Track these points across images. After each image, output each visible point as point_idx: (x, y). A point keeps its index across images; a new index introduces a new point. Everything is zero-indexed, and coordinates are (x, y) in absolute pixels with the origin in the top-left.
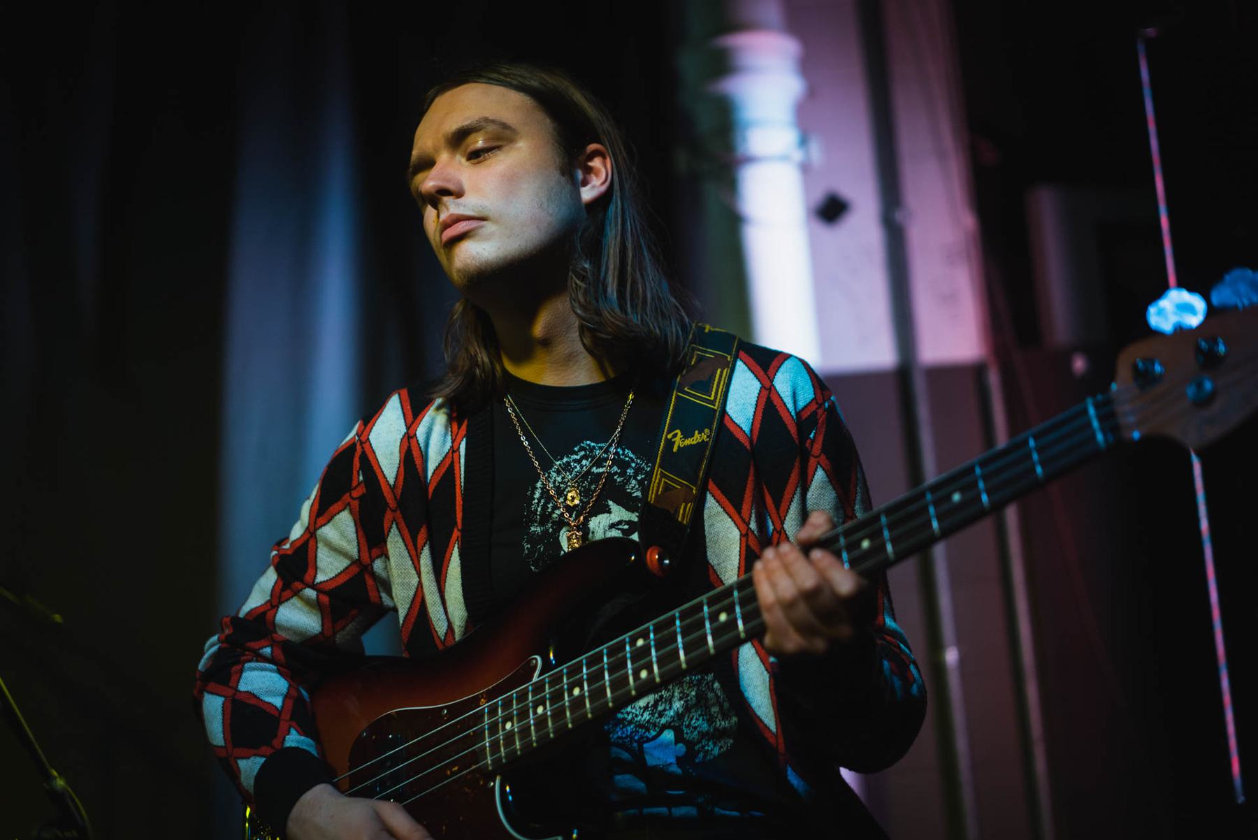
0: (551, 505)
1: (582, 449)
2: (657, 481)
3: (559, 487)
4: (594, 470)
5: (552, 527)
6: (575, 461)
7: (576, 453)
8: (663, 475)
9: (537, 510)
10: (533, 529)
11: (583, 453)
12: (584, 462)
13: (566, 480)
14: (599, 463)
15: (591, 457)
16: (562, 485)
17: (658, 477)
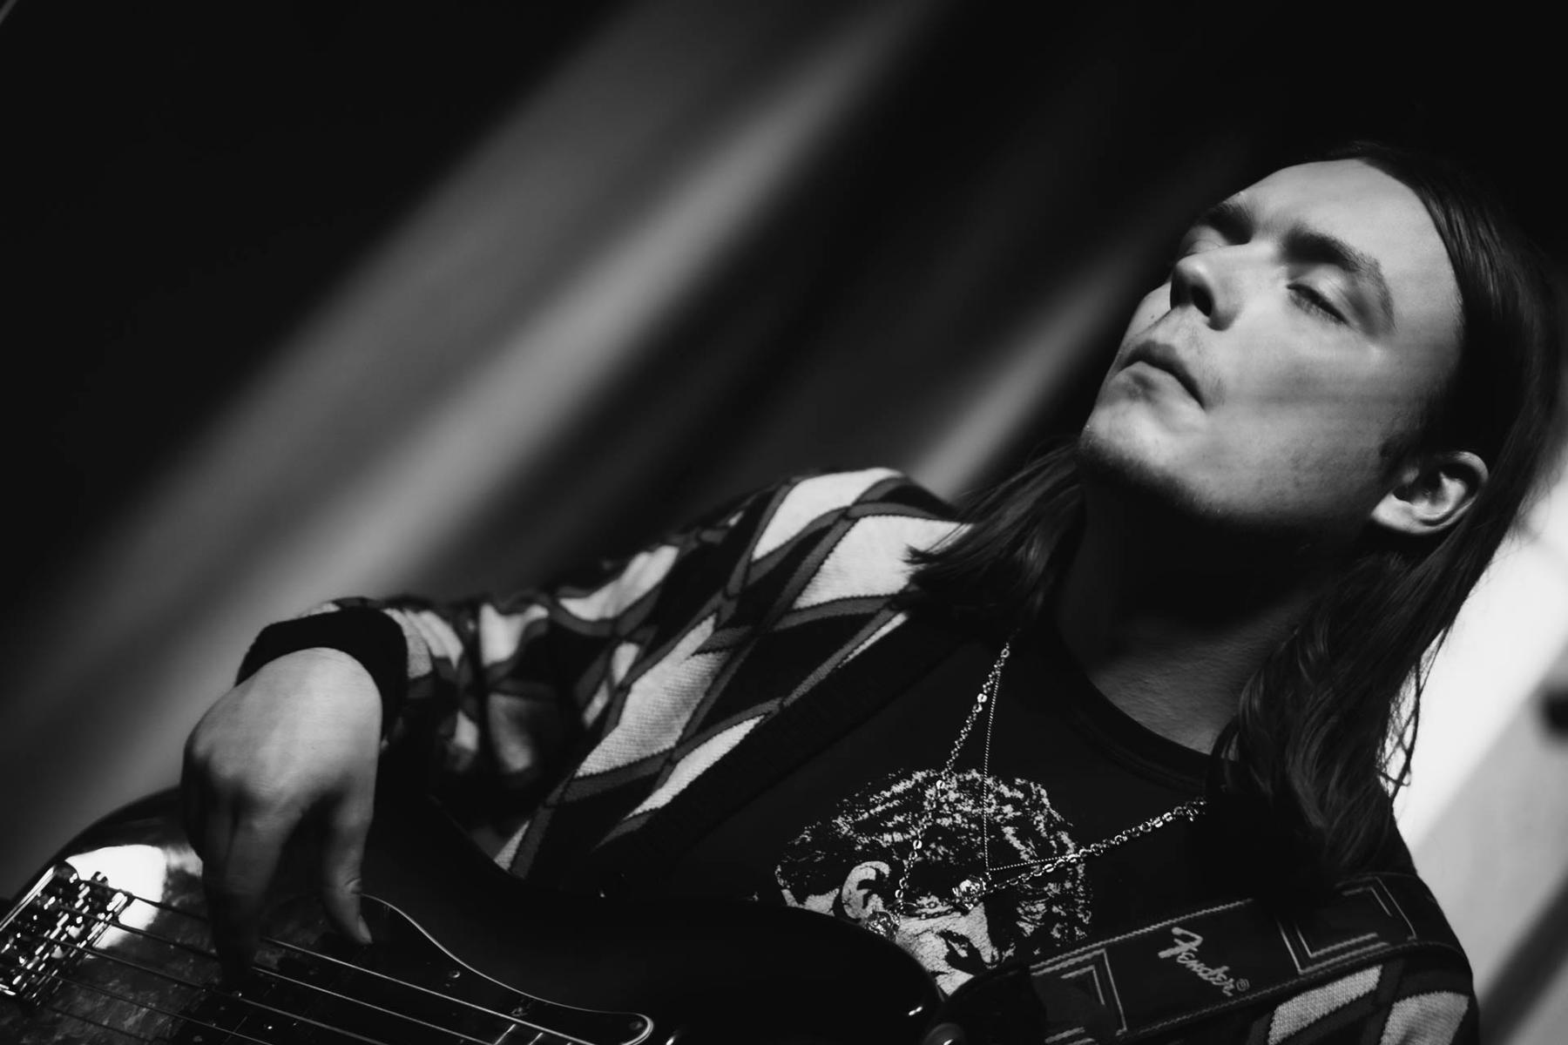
0: (901, 819)
1: (1025, 789)
2: (1080, 959)
3: (940, 805)
4: (1009, 831)
5: (865, 846)
6: (999, 796)
7: (1011, 787)
8: (1098, 961)
9: (875, 806)
10: (840, 821)
11: (1020, 795)
12: (1008, 809)
13: (960, 807)
14: (1025, 829)
15: (1025, 812)
16: (946, 807)
17: (1088, 956)
